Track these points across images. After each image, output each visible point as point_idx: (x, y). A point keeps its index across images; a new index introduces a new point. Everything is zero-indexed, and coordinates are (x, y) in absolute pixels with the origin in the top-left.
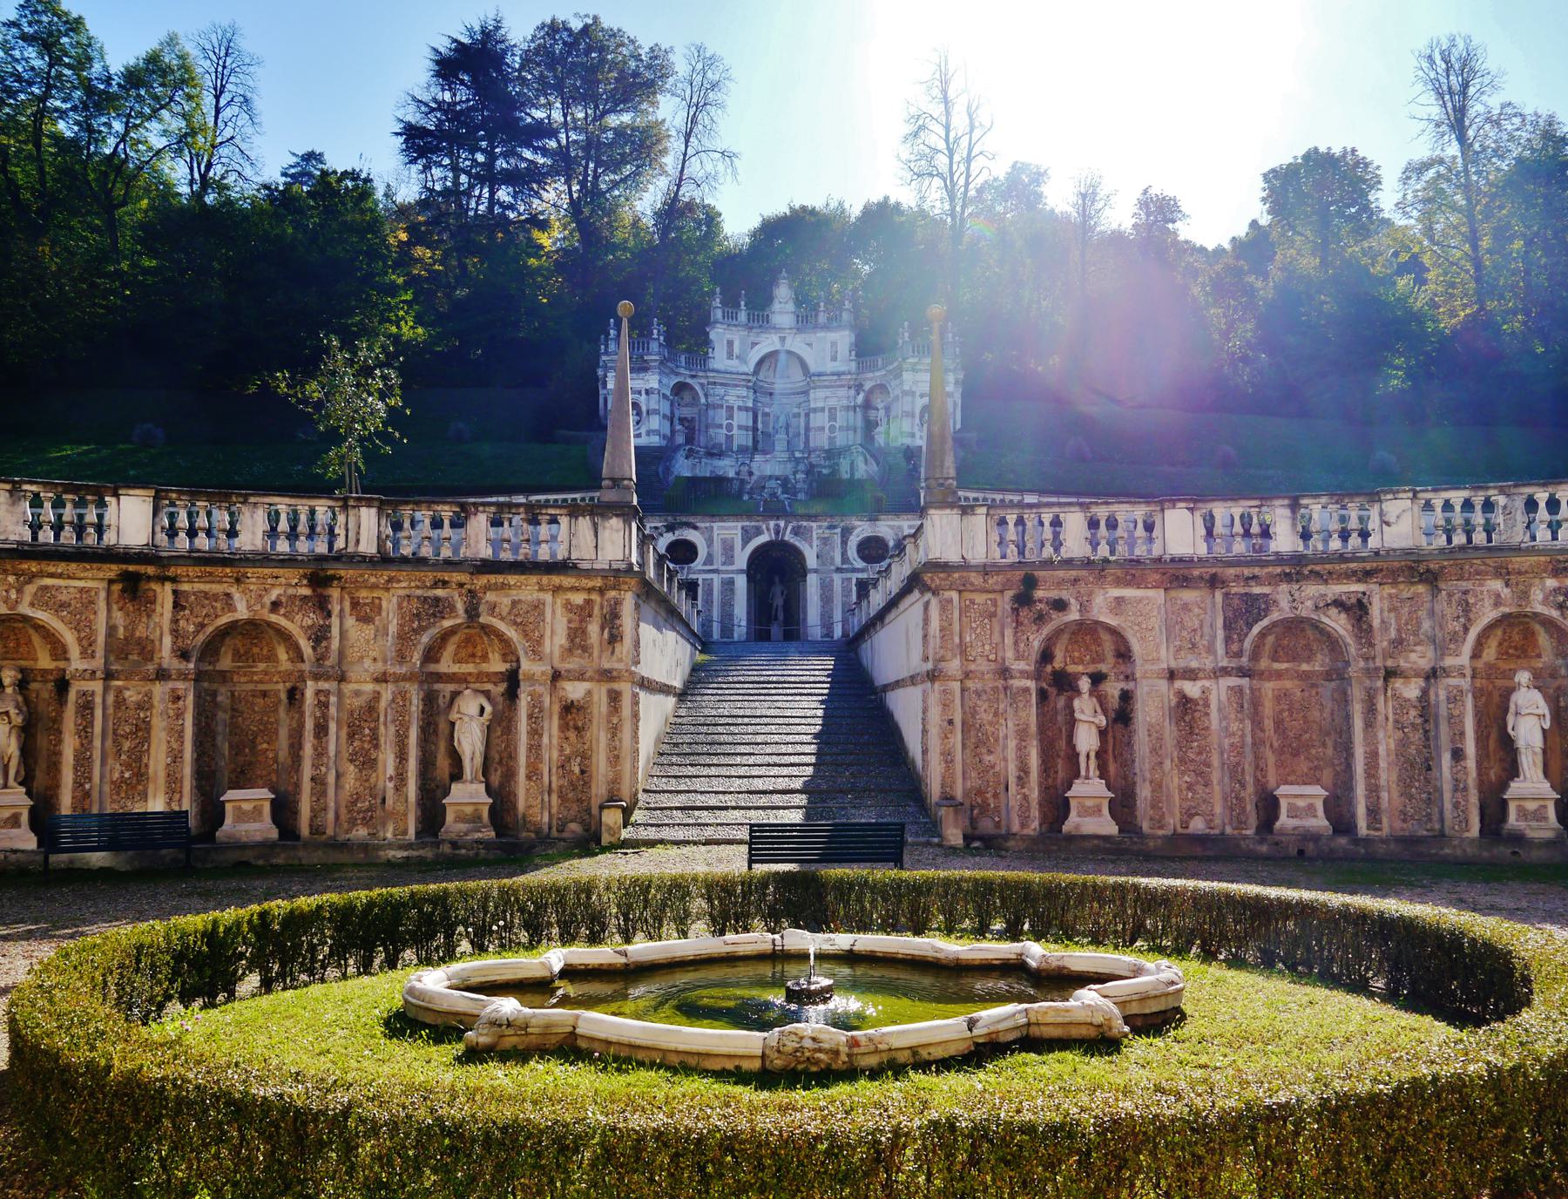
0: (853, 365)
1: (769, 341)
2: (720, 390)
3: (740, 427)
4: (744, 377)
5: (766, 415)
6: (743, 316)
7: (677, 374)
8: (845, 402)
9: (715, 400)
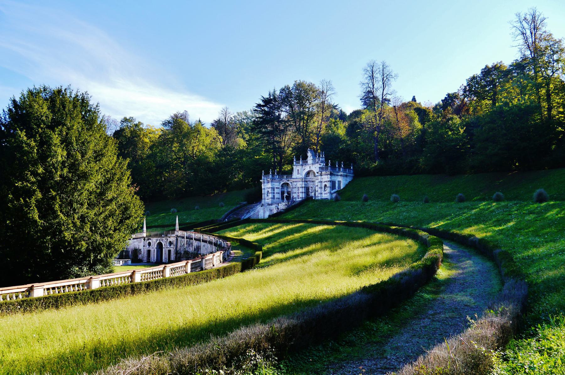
2: (295, 183)
5: (311, 187)
6: (301, 163)
7: (283, 181)
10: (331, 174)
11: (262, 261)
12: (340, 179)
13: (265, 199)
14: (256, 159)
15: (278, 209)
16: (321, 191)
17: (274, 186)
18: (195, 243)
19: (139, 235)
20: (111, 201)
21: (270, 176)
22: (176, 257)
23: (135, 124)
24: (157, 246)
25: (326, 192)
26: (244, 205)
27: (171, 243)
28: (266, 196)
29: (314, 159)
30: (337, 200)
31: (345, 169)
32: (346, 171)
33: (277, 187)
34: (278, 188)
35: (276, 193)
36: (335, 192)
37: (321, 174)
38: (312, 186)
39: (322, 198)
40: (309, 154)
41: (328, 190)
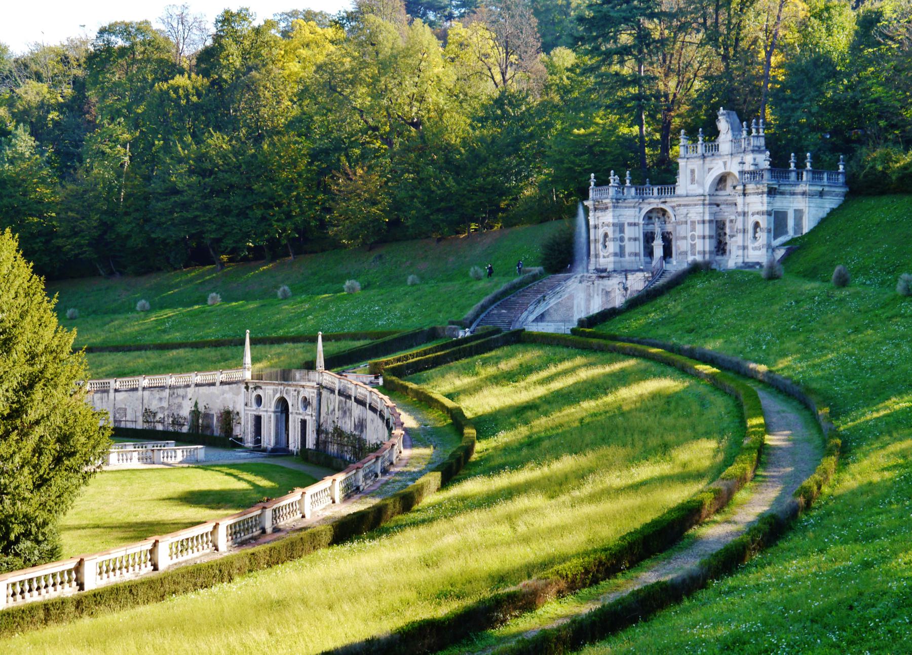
2: (683, 210)
3: (699, 237)
4: (698, 198)
5: (731, 221)
7: (649, 204)
9: (681, 218)
10: (772, 192)
11: (430, 498)
12: (800, 203)
13: (597, 256)
14: (579, 135)
15: (626, 289)
16: (744, 241)
17: (622, 219)
18: (357, 410)
19: (236, 375)
20: (37, 422)
21: (612, 191)
22: (318, 440)
23: (254, 29)
24: (277, 407)
25: (757, 244)
26: (535, 278)
27: (306, 403)
28: (600, 246)
29: (735, 140)
30: (772, 276)
31: (817, 172)
32: (821, 179)
33: (632, 221)
34: (635, 224)
35: (630, 239)
36: (783, 245)
37: (744, 190)
38: (733, 217)
39: (747, 260)
40: (723, 125)
41: (763, 237)
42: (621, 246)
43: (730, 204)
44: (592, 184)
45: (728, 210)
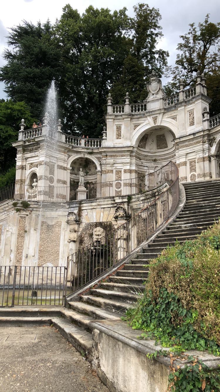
0: (206, 125)
1: (147, 122)
2: (110, 161)
3: (126, 185)
6: (127, 109)
7: (78, 152)
8: (201, 155)
42: (50, 187)
43: (149, 160)
44: (22, 127)
45: (148, 164)
